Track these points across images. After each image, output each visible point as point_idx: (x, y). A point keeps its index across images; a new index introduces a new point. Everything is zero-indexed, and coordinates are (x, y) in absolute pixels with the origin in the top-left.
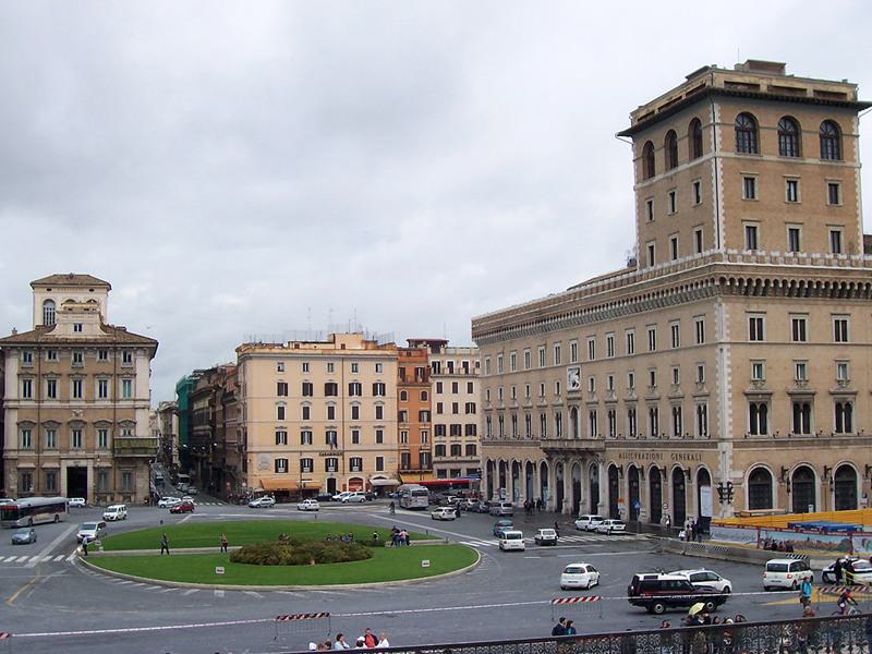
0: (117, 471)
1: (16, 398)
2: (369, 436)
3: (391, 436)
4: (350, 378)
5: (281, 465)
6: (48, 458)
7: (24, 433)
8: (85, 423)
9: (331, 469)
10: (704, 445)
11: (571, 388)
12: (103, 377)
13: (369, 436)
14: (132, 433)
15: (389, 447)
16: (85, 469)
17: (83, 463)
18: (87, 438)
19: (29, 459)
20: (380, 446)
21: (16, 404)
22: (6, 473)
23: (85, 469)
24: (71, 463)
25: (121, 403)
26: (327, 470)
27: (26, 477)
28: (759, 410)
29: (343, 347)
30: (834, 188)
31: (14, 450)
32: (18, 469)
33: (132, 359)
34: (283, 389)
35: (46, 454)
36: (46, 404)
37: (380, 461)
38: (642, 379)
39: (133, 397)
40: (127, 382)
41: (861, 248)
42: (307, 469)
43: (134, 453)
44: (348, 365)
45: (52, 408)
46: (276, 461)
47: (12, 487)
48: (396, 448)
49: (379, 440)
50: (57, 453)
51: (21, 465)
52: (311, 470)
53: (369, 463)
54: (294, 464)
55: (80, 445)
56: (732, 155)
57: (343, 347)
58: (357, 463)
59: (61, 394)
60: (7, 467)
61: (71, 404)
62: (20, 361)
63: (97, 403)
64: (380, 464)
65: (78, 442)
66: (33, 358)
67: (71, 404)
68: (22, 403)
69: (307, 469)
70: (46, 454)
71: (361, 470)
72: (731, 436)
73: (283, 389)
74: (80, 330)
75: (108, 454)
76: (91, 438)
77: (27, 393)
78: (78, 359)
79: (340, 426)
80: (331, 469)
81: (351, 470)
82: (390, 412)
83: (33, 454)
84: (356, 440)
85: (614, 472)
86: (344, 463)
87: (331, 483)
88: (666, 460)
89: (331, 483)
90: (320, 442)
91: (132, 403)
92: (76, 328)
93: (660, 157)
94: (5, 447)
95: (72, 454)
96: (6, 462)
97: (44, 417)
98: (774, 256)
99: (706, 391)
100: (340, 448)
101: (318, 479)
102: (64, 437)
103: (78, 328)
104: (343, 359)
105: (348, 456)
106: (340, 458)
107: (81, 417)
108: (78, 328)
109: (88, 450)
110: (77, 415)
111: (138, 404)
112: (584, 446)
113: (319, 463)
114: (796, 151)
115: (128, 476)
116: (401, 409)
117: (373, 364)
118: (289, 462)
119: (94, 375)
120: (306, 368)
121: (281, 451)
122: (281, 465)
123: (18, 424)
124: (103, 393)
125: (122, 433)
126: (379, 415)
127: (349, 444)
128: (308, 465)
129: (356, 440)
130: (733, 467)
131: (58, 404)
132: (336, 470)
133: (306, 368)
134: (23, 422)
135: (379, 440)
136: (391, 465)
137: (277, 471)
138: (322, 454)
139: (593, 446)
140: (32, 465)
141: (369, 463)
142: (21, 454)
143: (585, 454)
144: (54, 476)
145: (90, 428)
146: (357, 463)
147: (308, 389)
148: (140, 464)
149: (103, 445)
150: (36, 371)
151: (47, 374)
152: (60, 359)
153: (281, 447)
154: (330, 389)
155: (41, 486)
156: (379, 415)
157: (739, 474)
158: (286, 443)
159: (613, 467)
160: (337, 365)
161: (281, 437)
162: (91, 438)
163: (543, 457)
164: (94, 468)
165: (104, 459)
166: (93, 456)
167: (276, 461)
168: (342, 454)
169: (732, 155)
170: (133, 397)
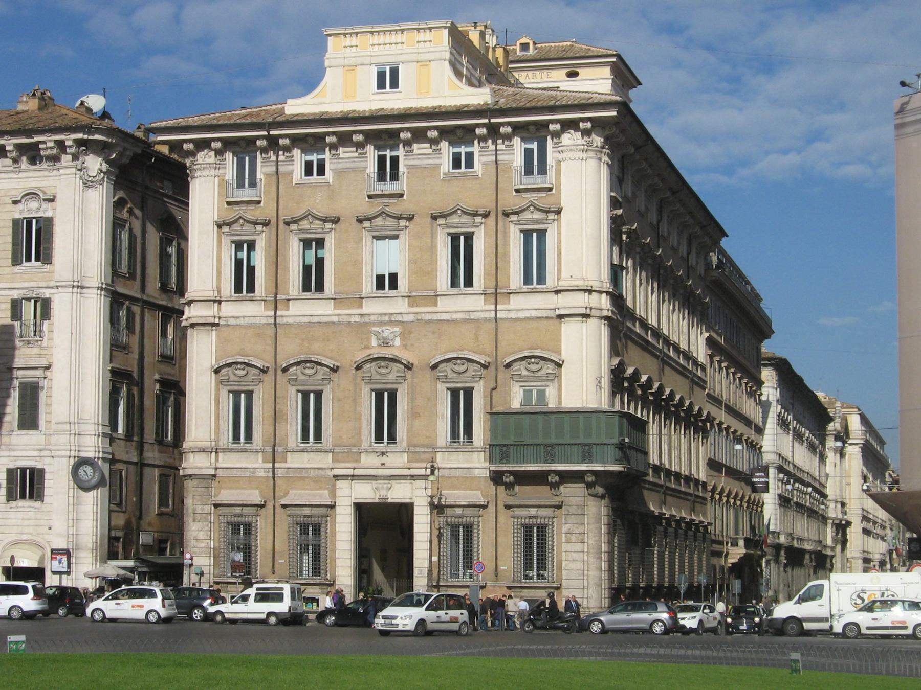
0: (504, 515)
1: (211, 295)
6: (300, 476)
7: (237, 394)
8: (409, 367)
12: (460, 223)
14: (550, 392)
16: (404, 511)
17: (398, 493)
18: (414, 414)
19: (251, 479)
22: (189, 520)
23: (404, 511)
24: (366, 493)
25: (516, 302)
31: (203, 450)
33: (550, 160)
35: (295, 461)
39: (551, 281)
40: (534, 240)
43: (550, 458)
50: (325, 460)
51: (226, 496)
55: (392, 437)
59: (339, 281)
60: (189, 502)
61: (369, 307)
62: (223, 184)
63: (443, 304)
65: (385, 428)
66: (259, 175)
67: (369, 307)
68: (228, 310)
70: (295, 461)
74: (395, 84)
75: (475, 462)
76: (426, 412)
77: (244, 279)
78: (388, 170)
92: (381, 76)
95: (369, 462)
96: (189, 484)
97: (290, 350)
102: (349, 411)
103: (388, 78)
107: (396, 349)
108: (388, 78)
109: (413, 452)
110: (385, 343)
119: (434, 218)
124: (462, 272)
140: (255, 497)
142: (227, 461)
144: (317, 529)
145: (424, 380)
148: (572, 493)
149: (461, 428)
150: (266, 210)
151: (295, 221)
152: (338, 173)
162: (426, 412)
164: (437, 508)
165: (466, 481)
166: (436, 470)
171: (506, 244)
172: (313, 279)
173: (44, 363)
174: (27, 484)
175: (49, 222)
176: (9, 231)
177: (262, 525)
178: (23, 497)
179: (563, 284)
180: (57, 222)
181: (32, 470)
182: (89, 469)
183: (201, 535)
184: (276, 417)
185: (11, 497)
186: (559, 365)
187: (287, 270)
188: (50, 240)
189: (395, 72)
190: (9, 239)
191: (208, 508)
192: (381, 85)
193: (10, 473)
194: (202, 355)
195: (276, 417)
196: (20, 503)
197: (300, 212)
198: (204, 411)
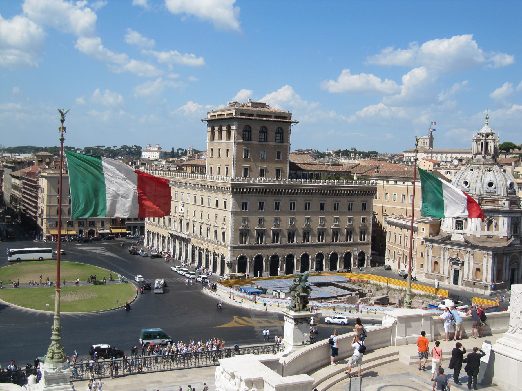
10: (223, 246)
11: (180, 211)
26: (79, 226)
28: (244, 234)
30: (279, 154)
38: (205, 216)
41: (288, 176)
56: (241, 141)
72: (233, 245)
85: (193, 246)
88: (211, 248)
93: (216, 134)
98: (254, 180)
99: (225, 227)
106: (85, 221)
112: (183, 236)
114: (266, 140)
130: (233, 256)
139: (186, 237)
143: (182, 239)
157: (235, 258)
159: (193, 246)
163: (169, 235)
169: (241, 141)
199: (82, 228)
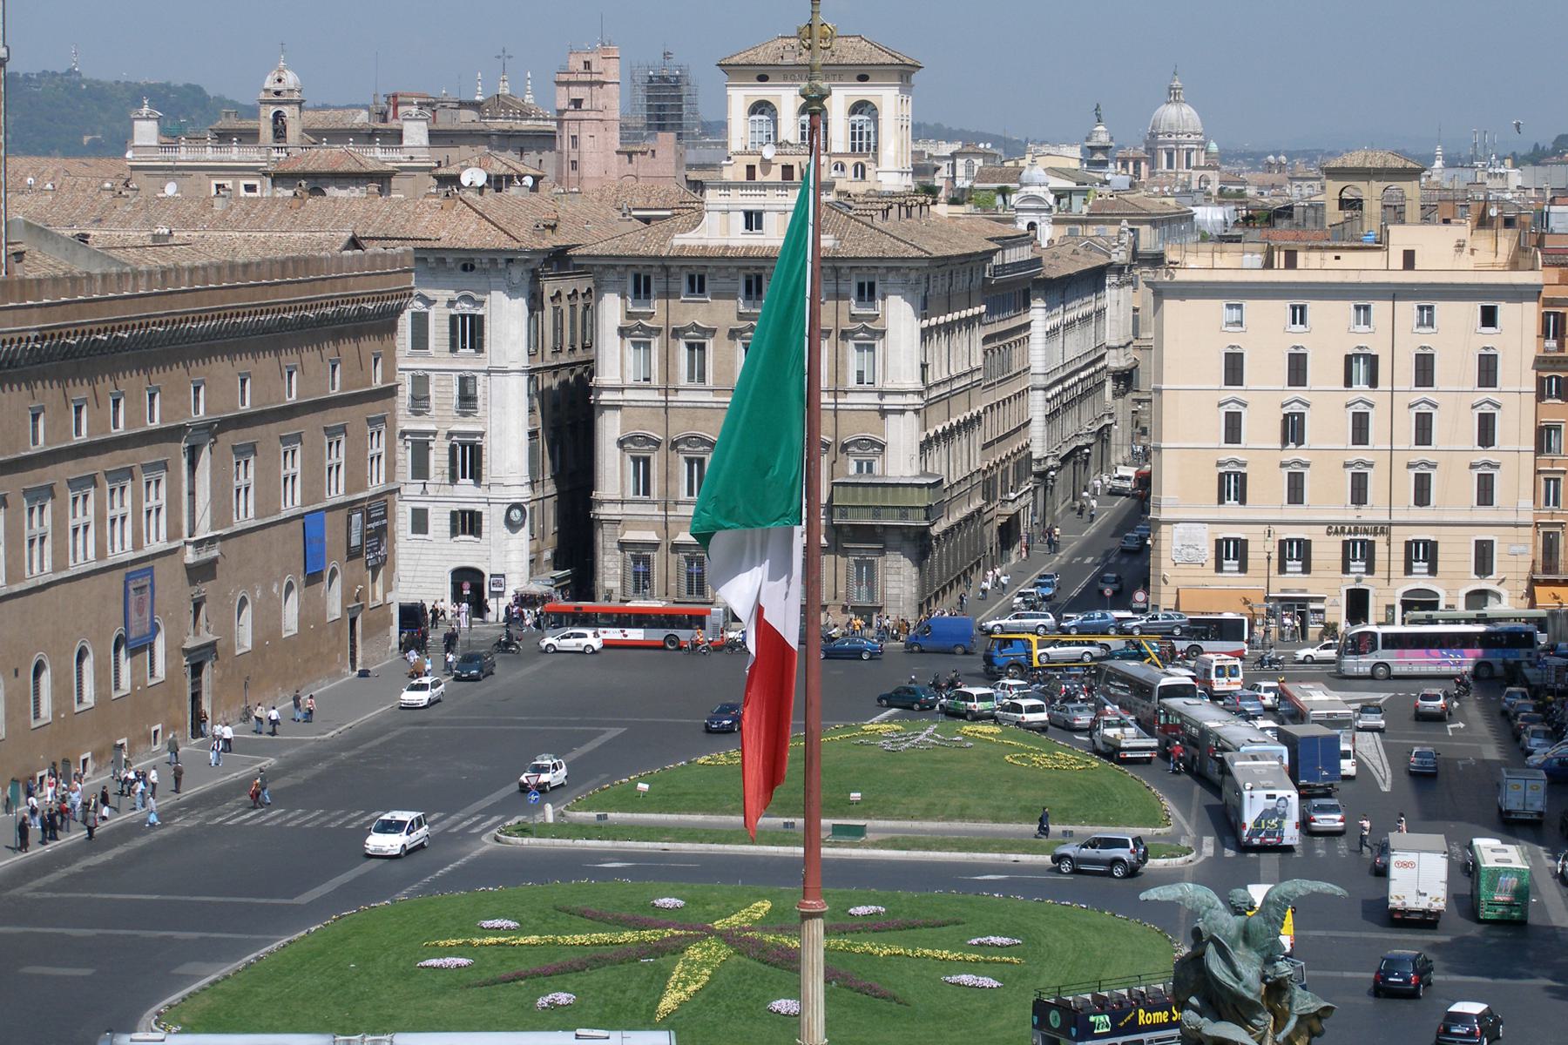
1: (618, 383)
2: (1454, 490)
3: (1517, 492)
4: (1411, 341)
5: (1232, 551)
7: (636, 460)
9: (1358, 566)
13: (1454, 490)
14: (877, 466)
15: (1510, 518)
20: (1485, 514)
21: (619, 396)
22: (600, 553)
27: (639, 555)
29: (1409, 259)
31: (612, 501)
32: (623, 546)
34: (1234, 368)
36: (682, 396)
37: (1484, 557)
42: (1294, 566)
44: (1408, 310)
45: (695, 407)
46: (1218, 542)
47: (609, 584)
48: (1529, 519)
49: (1485, 493)
51: (631, 536)
52: (1307, 569)
53: (1457, 553)
54: (1261, 548)
57: (1409, 259)
58: (1425, 553)
64: (1484, 557)
68: (629, 395)
69: (1294, 566)
71: (1433, 570)
73: (1234, 368)
74: (759, 227)
79: (1381, 461)
80: (1358, 566)
81: (1408, 570)
82: (1515, 429)
83: (655, 510)
84: (1422, 494)
86: (1388, 553)
87: (1358, 604)
89: (1358, 604)
90: (1329, 498)
91: (873, 399)
94: (598, 494)
97: (679, 428)
100: (1373, 512)
101: (1327, 586)
103: (753, 220)
104: (1395, 293)
105: (1400, 536)
108: (753, 220)
111: (889, 401)
113: (1327, 550)
115: (866, 574)
116: (1546, 419)
117: (1474, 309)
118: (1250, 547)
120: (1299, 314)
121: (1233, 519)
122: (1232, 551)
123: (621, 443)
125: (853, 469)
126: (1487, 430)
127: (1406, 509)
128: (1297, 552)
129: (1422, 494)
131: (709, 397)
132: (1370, 569)
133: (1299, 314)
134: (632, 439)
135: (1485, 493)
136: (1516, 557)
137: (1219, 568)
138: (1334, 528)
140: (652, 536)
141: (1457, 553)
142: (628, 509)
146: (1425, 553)
147: (1297, 369)
151: (685, 330)
153: (1232, 509)
154: (1362, 367)
155: (672, 584)
156: (1486, 432)
158: (1242, 499)
160: (1380, 308)
161: (1233, 486)
167: (1218, 542)
168: (1384, 529)
170: (878, 385)
171: (845, 354)
172: (698, 373)
173: (480, 429)
174: (467, 523)
175: (481, 318)
176: (447, 323)
177: (656, 557)
178: (464, 532)
179: (889, 386)
180: (487, 318)
181: (472, 513)
182: (518, 512)
183: (611, 565)
184: (667, 477)
185: (454, 532)
186: (882, 447)
187: (676, 366)
188: (482, 333)
189: (759, 214)
190: (448, 330)
191: (615, 545)
192: (749, 226)
193: (453, 514)
194: (610, 429)
195: (667, 477)
196: (462, 537)
197: (687, 322)
198: (613, 473)
199: (1367, 583)
